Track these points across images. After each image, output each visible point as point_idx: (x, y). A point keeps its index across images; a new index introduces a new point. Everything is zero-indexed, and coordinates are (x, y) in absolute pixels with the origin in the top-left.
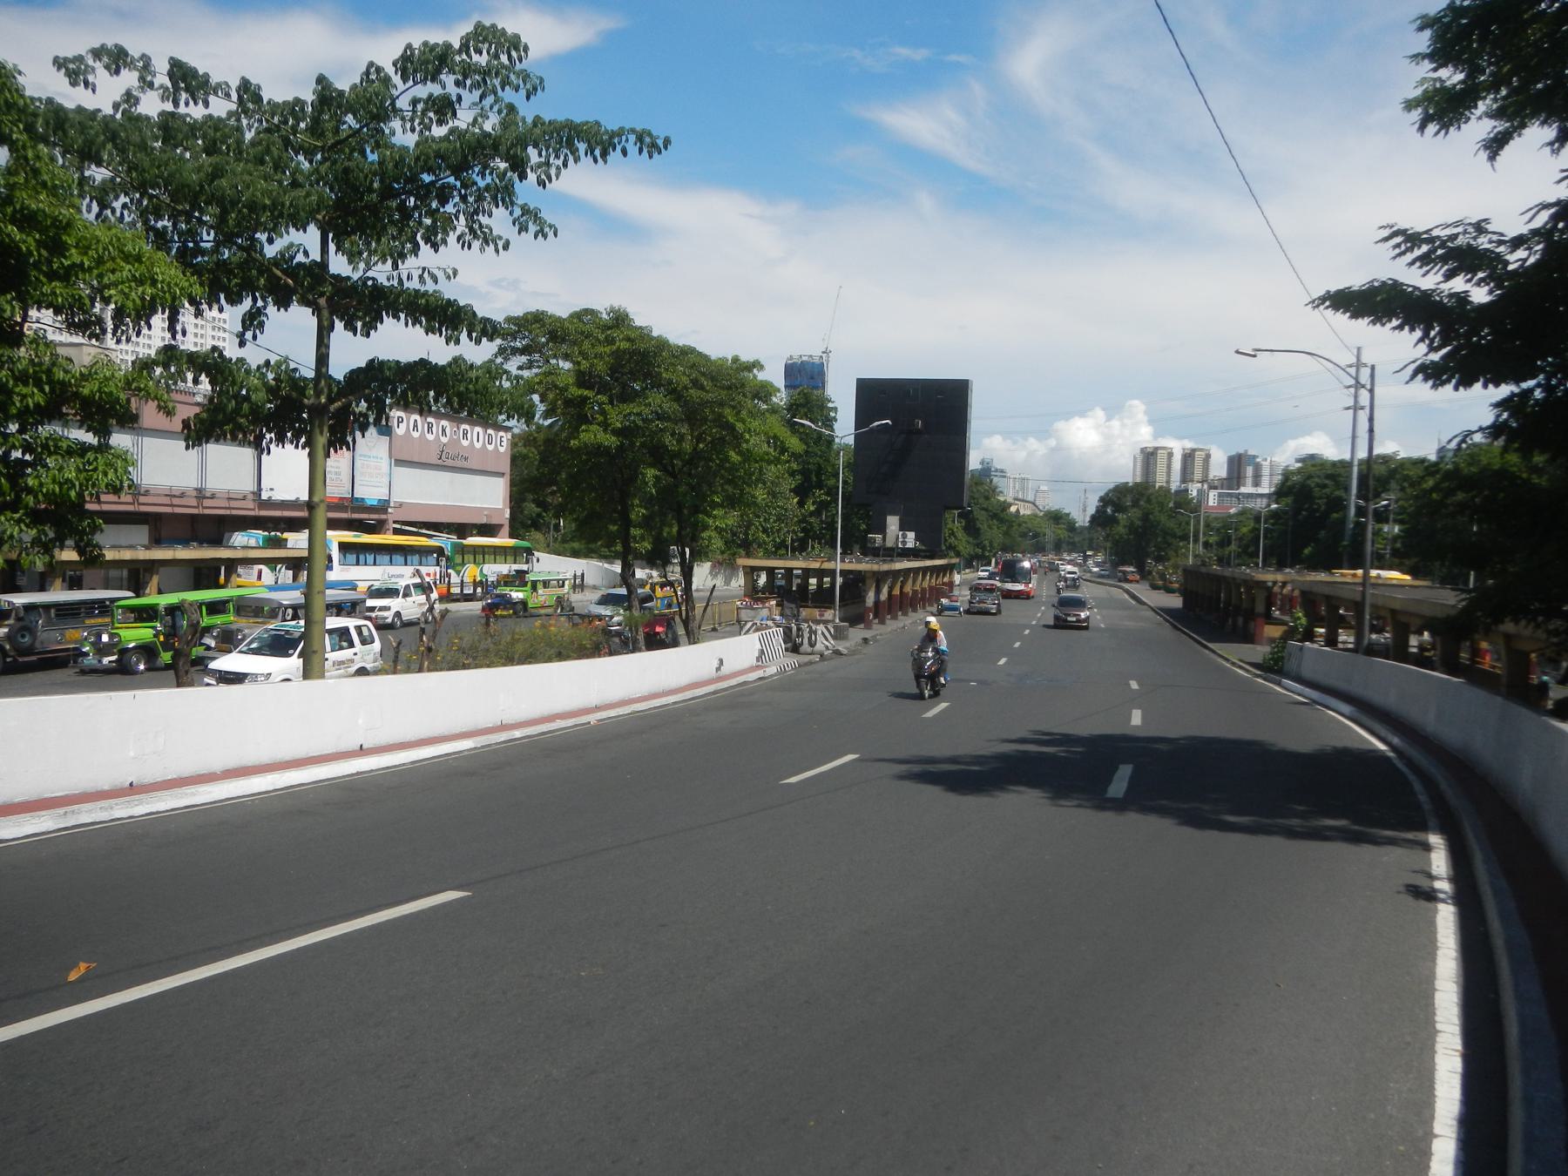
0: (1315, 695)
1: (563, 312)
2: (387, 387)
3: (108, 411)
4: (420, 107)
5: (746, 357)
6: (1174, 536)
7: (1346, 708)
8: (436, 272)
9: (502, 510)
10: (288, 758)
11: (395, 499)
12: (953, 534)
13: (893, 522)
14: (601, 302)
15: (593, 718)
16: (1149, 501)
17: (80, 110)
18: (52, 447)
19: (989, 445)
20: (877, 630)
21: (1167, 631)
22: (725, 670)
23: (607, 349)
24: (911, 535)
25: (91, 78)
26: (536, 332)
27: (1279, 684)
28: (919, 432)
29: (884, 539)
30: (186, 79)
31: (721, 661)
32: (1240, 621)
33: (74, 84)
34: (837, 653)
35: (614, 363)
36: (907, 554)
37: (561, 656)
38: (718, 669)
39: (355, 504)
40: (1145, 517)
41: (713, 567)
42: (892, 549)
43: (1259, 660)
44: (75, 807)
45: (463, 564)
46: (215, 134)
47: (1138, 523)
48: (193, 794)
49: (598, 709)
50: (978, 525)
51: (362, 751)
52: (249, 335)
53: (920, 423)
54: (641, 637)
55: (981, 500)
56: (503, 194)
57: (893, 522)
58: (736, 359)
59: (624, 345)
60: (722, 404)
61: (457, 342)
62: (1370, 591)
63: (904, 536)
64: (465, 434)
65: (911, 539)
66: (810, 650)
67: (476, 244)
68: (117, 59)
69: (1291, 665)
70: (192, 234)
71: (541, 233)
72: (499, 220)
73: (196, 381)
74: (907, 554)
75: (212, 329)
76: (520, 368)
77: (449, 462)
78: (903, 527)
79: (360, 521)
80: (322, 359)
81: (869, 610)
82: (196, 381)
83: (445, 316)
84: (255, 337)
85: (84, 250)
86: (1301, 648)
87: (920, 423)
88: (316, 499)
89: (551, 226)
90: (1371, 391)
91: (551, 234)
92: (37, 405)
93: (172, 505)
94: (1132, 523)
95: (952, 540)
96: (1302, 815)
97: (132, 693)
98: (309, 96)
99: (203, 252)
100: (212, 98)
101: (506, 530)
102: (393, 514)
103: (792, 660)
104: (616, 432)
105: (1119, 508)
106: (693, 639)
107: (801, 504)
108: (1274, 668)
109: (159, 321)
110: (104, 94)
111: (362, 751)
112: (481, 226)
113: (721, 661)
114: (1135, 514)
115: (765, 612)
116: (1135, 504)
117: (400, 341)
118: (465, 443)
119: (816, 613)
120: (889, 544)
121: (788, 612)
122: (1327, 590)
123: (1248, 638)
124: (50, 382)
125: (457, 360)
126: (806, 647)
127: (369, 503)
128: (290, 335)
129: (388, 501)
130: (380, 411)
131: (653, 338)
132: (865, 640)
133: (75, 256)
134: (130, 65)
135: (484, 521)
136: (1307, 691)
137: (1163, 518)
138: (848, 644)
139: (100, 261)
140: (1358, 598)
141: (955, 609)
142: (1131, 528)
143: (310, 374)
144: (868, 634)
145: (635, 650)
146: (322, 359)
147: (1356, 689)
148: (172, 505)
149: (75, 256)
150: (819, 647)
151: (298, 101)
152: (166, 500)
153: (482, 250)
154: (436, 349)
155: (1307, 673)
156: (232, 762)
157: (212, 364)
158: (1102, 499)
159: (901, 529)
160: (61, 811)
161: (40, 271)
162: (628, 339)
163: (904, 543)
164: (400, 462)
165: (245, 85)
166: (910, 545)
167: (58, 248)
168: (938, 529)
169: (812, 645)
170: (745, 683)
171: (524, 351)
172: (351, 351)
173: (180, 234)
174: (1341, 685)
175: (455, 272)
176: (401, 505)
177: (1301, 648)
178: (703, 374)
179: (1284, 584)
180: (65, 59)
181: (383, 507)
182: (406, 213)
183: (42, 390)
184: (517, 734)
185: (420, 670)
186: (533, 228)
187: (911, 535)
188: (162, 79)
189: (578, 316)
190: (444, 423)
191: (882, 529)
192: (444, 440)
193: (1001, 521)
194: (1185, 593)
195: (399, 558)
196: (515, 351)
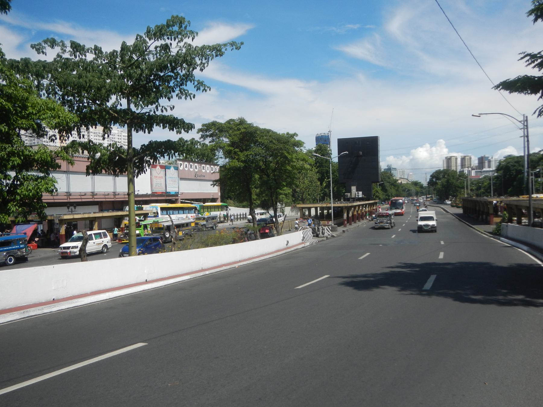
0: (513, 243)
1: (222, 121)
2: (155, 149)
3: (48, 164)
4: (158, 49)
5: (291, 132)
6: (459, 187)
7: (526, 248)
8: (167, 107)
9: (217, 193)
10: (116, 286)
11: (180, 192)
12: (377, 191)
13: (354, 189)
14: (235, 116)
15: (236, 265)
16: (448, 175)
17: (39, 61)
18: (26, 179)
19: (386, 160)
20: (348, 227)
21: (457, 222)
22: (290, 245)
23: (238, 132)
24: (361, 193)
25: (44, 50)
26: (212, 129)
27: (499, 239)
28: (361, 156)
29: (351, 195)
30: (77, 48)
31: (288, 242)
32: (484, 216)
33: (39, 53)
34: (333, 236)
35: (243, 137)
37: (227, 243)
38: (287, 245)
39: (167, 194)
40: (448, 181)
41: (292, 208)
42: (353, 198)
43: (491, 231)
44: (28, 310)
45: (204, 212)
46: (88, 67)
47: (445, 183)
48: (76, 302)
49: (240, 261)
50: (387, 188)
51: (147, 282)
52: (106, 135)
53: (361, 153)
54: (258, 234)
55: (387, 179)
56: (189, 77)
57: (354, 189)
58: (288, 134)
59: (243, 130)
60: (281, 149)
61: (180, 133)
62: (532, 202)
63: (358, 193)
64: (203, 168)
65: (360, 194)
66: (322, 236)
67: (183, 97)
68: (53, 43)
69: (503, 232)
70: (81, 101)
71: (205, 90)
72: (190, 87)
73: (83, 153)
74: (359, 199)
75: (94, 134)
76: (210, 142)
77: (199, 178)
78: (358, 190)
79: (170, 200)
80: (130, 142)
81: (345, 220)
82: (83, 153)
83: (174, 123)
84: (108, 136)
85: (33, 107)
86: (507, 226)
87: (361, 153)
88: (130, 192)
89: (208, 87)
91: (208, 90)
92: (18, 164)
95: (377, 194)
96: (505, 295)
97: (52, 266)
98: (119, 49)
99: (85, 107)
100: (87, 54)
101: (219, 200)
102: (180, 197)
103: (316, 240)
104: (242, 161)
105: (438, 179)
106: (279, 234)
107: (321, 184)
108: (497, 233)
109: (74, 132)
110: (50, 55)
111: (147, 282)
112: (184, 90)
113: (288, 242)
114: (444, 180)
116: (444, 177)
117: (160, 134)
118: (204, 171)
119: (326, 222)
120: (353, 196)
121: (316, 223)
122: (516, 203)
123: (487, 223)
124: (23, 155)
125: (181, 139)
126: (321, 235)
127: (172, 193)
128: (119, 134)
129: (178, 193)
130: (155, 159)
131: (254, 127)
132: (344, 231)
133: (30, 110)
134: (58, 45)
135: (211, 197)
136: (510, 242)
137: (454, 181)
138: (337, 233)
139: (39, 111)
140: (528, 205)
142: (443, 186)
143: (126, 147)
144: (345, 229)
145: (256, 239)
146: (130, 142)
147: (529, 240)
148: (81, 199)
149: (30, 110)
150: (326, 234)
151: (114, 51)
152: (103, 197)
153: (186, 99)
154: (172, 136)
155: (510, 235)
156: (95, 289)
157: (90, 147)
158: (431, 176)
159: (357, 191)
160: (22, 311)
161: (18, 116)
162: (245, 128)
163: (358, 196)
164: (182, 179)
165: (96, 48)
166: (360, 196)
167: (25, 107)
169: (323, 234)
171: (211, 136)
172: (141, 139)
173: (77, 101)
174: (523, 239)
175: (174, 107)
176: (182, 193)
178: (274, 139)
179: (501, 202)
180: (35, 45)
181: (176, 194)
182: (157, 88)
183: (20, 159)
184: (207, 272)
185: (171, 251)
186: (202, 88)
187: (361, 193)
188: (69, 49)
189: (229, 122)
190: (196, 164)
191: (350, 191)
192: (196, 170)
193: (395, 186)
194: (464, 208)
195: (181, 212)
196: (207, 136)
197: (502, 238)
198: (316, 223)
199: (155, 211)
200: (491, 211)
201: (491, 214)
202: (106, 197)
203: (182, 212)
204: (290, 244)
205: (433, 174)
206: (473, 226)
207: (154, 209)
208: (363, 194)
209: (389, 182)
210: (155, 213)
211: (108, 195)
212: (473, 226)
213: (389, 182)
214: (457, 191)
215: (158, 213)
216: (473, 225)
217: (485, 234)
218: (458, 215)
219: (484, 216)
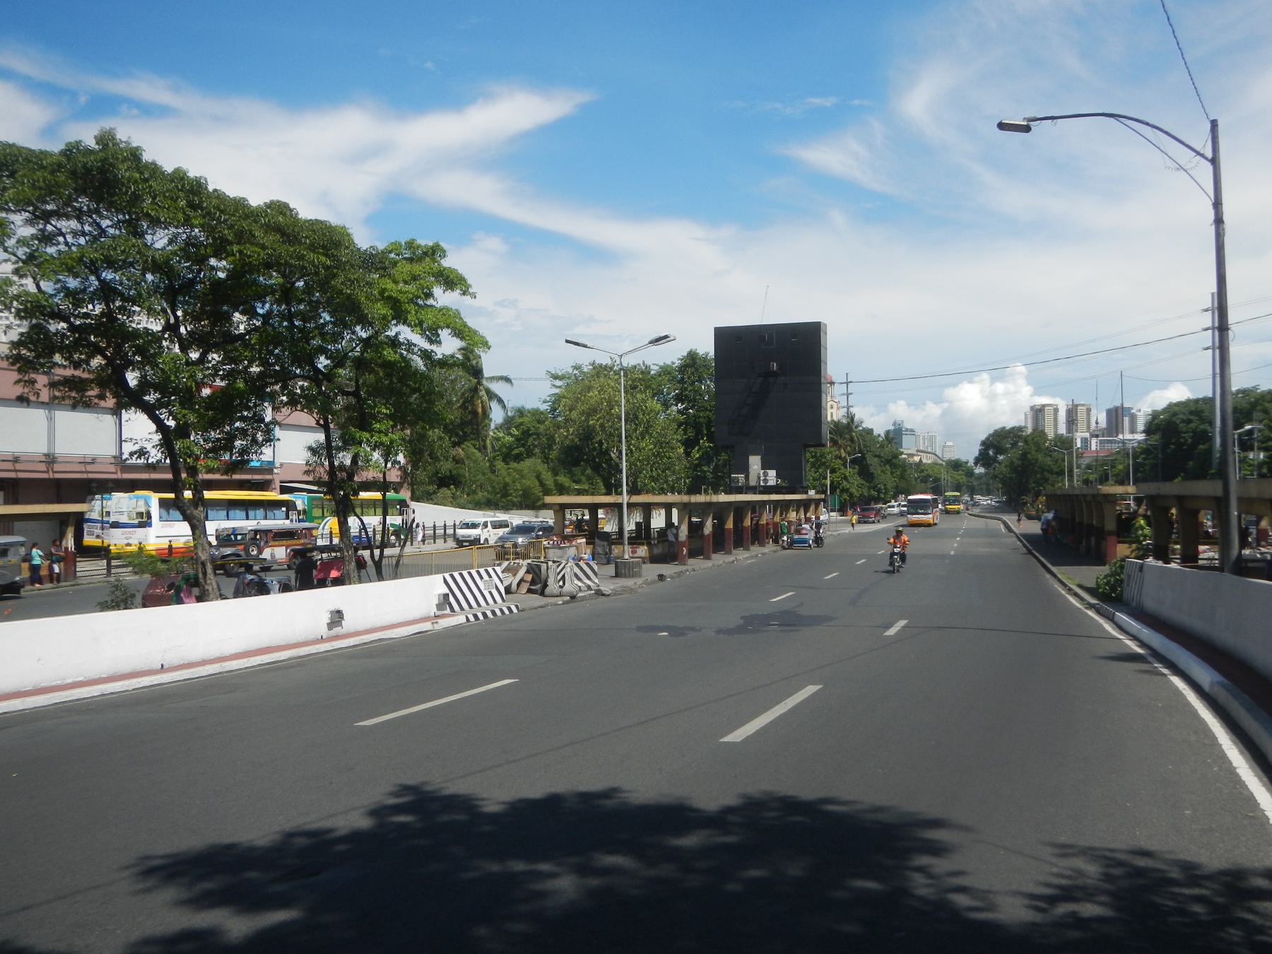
6: (1051, 472)
7: (1205, 675)
12: (845, 478)
13: (755, 462)
24: (772, 473)
27: (1111, 619)
28: (774, 374)
29: (747, 478)
32: (1093, 540)
36: (768, 490)
40: (1024, 456)
43: (1092, 584)
45: (323, 517)
47: (1017, 462)
50: (872, 469)
57: (755, 462)
63: (766, 475)
69: (1130, 592)
74: (768, 490)
78: (765, 466)
79: (248, 481)
81: (683, 544)
86: (1141, 568)
90: (1214, 161)
93: (16, 471)
94: (1012, 463)
102: (278, 476)
105: (1000, 450)
107: (687, 454)
114: (1014, 455)
115: (572, 552)
116: (1014, 445)
120: (752, 483)
123: (1100, 559)
126: (553, 586)
129: (273, 463)
132: (661, 577)
137: (1040, 457)
138: (640, 581)
141: (805, 541)
142: (1011, 465)
147: (1225, 636)
152: (9, 466)
155: (1150, 604)
158: (983, 443)
163: (766, 481)
168: (799, 468)
170: (381, 640)
176: (282, 465)
177: (1141, 568)
187: (772, 473)
191: (745, 469)
197: (1122, 617)
198: (600, 550)
199: (143, 510)
200: (1110, 525)
201: (1110, 533)
202: (89, 468)
203: (243, 514)
204: (348, 624)
205: (987, 439)
206: (1053, 569)
207: (141, 503)
208: (778, 476)
209: (879, 456)
210: (140, 515)
211: (93, 461)
212: (1053, 569)
213: (879, 456)
214: (1047, 480)
215: (149, 516)
216: (1054, 565)
217: (1076, 595)
218: (1029, 539)
219: (1093, 540)
